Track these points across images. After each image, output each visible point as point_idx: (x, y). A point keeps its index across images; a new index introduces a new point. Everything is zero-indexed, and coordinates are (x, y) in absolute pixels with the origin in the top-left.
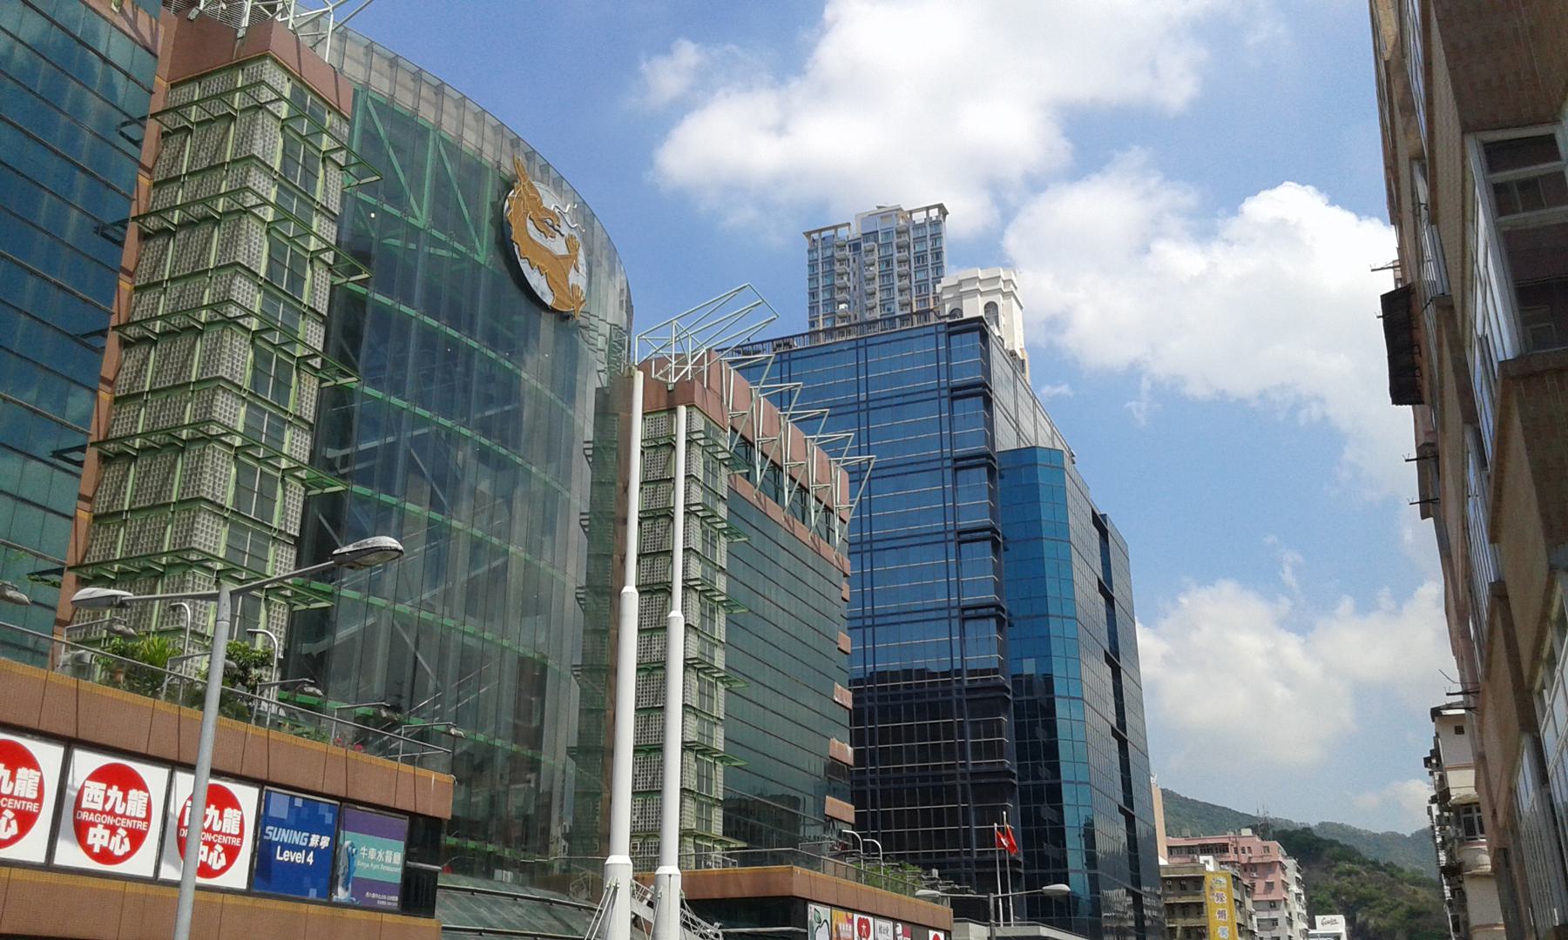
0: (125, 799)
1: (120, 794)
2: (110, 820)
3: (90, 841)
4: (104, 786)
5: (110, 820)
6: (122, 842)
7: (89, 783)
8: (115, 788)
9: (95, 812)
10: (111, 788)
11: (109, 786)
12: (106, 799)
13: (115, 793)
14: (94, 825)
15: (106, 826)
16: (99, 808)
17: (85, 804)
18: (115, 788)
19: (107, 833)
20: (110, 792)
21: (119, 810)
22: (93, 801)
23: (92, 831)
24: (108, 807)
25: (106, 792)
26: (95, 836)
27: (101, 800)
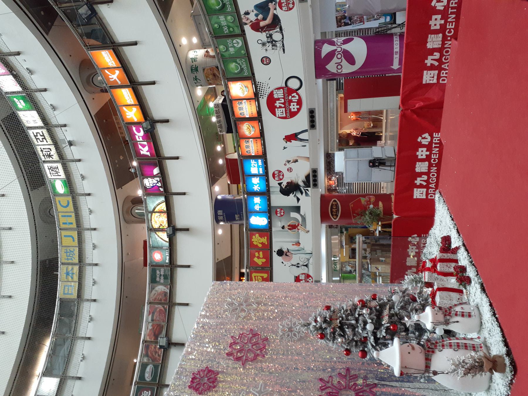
0: (278, 99)
1: (278, 102)
2: (287, 104)
3: (296, 110)
4: (276, 109)
5: (287, 104)
6: (294, 97)
7: (277, 116)
8: (276, 104)
9: (286, 111)
10: (276, 106)
11: (276, 107)
12: (280, 107)
13: (277, 104)
14: (290, 109)
15: (290, 105)
16: (284, 109)
17: (284, 115)
18: (276, 104)
19: (292, 104)
20: (278, 106)
21: (283, 101)
22: (283, 113)
23: (293, 110)
24: (283, 106)
25: (278, 108)
26: (294, 109)
27: (281, 109)
